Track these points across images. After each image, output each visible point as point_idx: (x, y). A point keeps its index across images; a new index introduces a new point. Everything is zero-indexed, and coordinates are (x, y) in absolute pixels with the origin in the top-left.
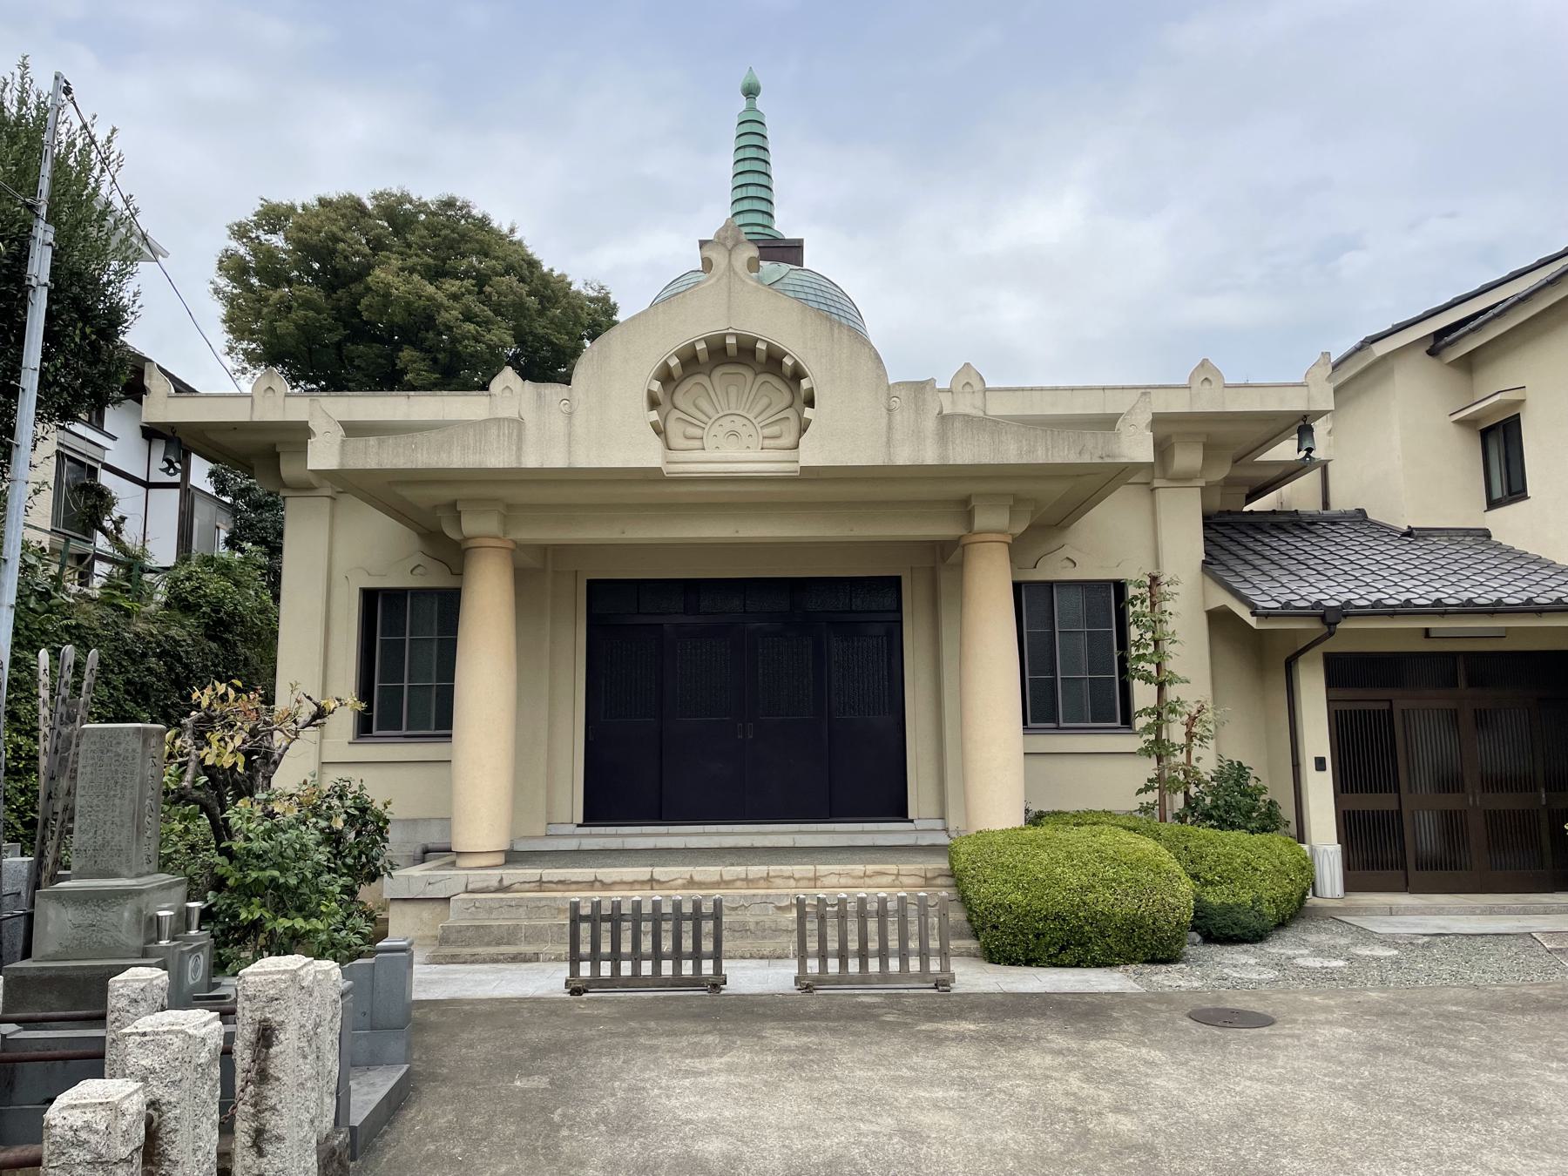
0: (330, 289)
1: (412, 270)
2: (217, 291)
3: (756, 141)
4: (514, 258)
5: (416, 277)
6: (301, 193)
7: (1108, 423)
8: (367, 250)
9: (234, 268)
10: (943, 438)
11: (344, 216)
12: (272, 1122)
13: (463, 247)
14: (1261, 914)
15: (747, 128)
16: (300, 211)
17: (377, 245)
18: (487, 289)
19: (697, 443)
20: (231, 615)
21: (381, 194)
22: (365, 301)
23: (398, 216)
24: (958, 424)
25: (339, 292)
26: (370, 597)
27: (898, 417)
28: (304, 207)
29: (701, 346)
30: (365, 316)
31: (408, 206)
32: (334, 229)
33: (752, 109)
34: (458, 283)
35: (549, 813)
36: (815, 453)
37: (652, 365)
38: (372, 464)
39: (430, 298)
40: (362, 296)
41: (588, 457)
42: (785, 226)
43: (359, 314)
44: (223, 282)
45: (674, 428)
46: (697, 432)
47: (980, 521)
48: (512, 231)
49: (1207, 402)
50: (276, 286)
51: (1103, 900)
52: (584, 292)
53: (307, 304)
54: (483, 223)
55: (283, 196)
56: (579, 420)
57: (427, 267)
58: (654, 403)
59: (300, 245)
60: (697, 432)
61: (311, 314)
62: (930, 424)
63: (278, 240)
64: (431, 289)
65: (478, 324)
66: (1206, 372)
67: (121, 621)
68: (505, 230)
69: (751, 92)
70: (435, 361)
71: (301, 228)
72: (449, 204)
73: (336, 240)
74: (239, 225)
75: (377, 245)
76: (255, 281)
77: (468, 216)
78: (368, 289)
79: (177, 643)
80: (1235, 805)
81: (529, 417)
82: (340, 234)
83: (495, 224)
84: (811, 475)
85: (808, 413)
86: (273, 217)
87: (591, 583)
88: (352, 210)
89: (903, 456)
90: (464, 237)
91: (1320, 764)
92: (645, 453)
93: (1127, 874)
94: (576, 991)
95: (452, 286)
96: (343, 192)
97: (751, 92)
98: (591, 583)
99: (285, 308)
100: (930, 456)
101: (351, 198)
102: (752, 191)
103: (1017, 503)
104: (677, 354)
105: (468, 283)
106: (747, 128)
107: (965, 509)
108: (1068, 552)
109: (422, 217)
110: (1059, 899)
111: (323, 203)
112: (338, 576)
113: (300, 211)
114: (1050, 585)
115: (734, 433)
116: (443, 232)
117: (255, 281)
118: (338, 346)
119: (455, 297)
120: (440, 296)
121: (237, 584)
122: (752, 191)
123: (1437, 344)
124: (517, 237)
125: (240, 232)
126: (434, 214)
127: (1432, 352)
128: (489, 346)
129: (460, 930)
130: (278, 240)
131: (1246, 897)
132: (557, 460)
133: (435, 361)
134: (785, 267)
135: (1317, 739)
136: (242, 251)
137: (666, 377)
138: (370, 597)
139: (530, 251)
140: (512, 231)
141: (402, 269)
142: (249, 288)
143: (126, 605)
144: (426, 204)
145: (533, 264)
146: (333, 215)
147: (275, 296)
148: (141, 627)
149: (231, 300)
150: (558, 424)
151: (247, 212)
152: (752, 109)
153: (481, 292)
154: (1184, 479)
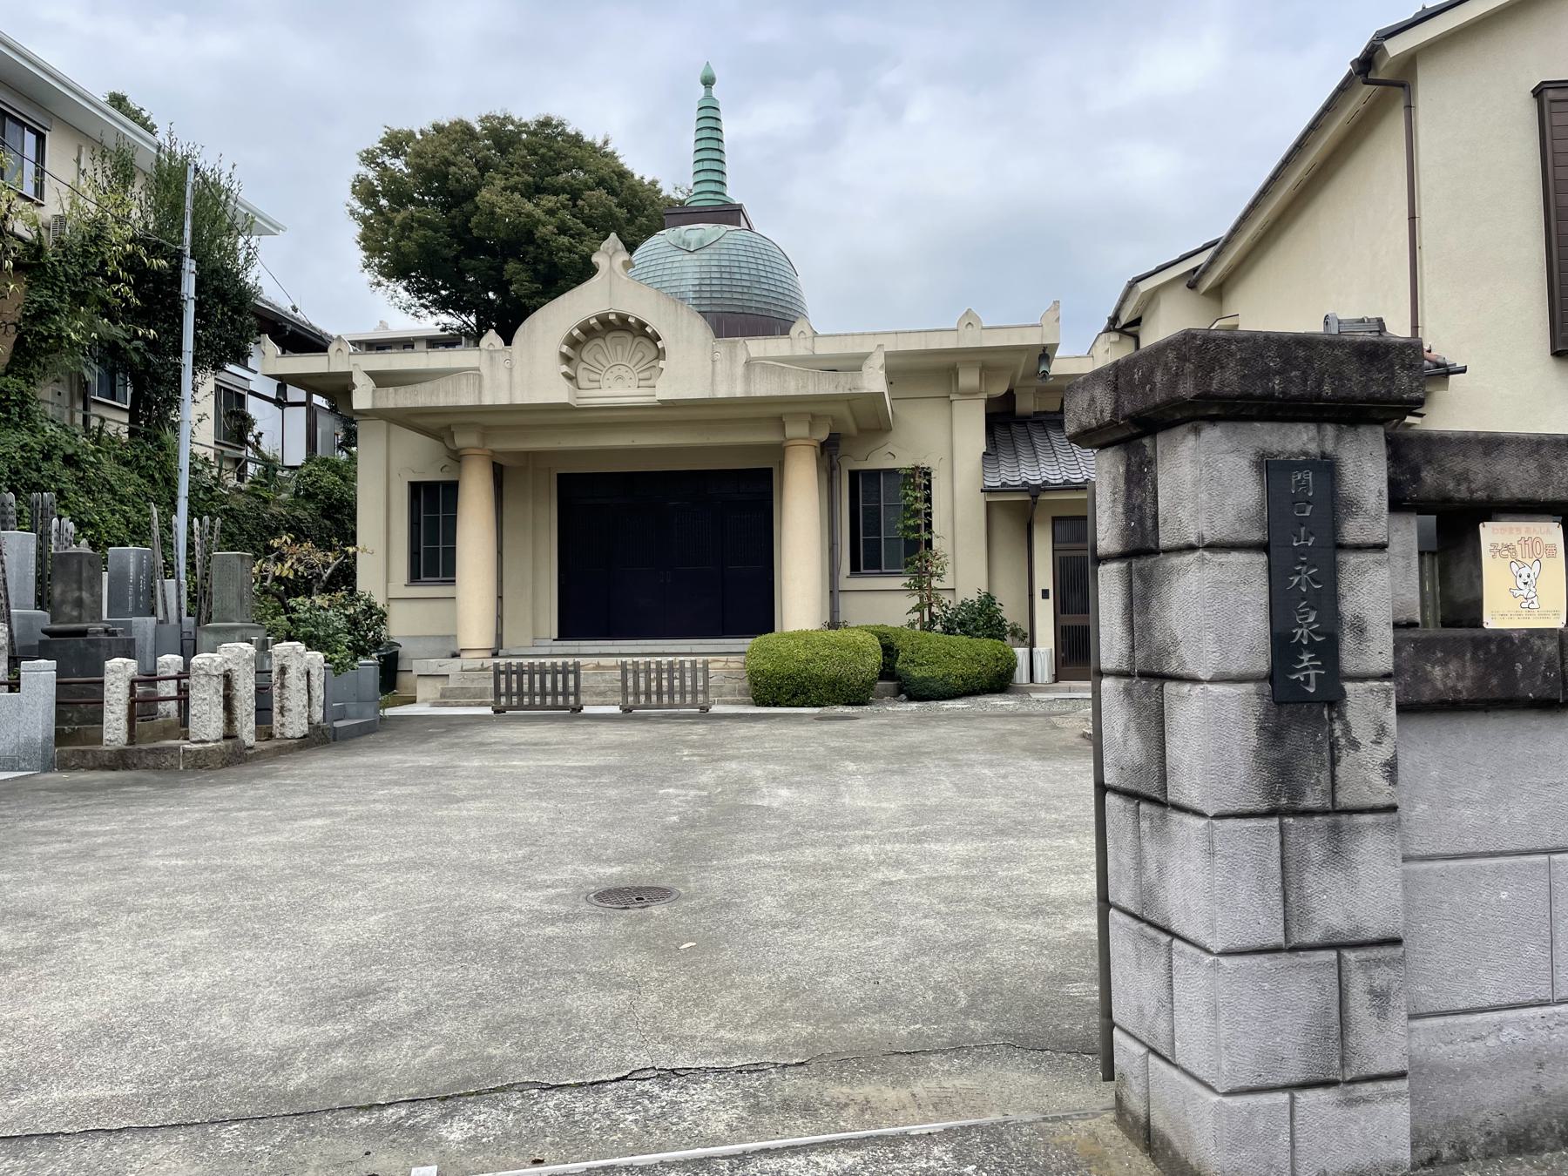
0: (446, 208)
1: (514, 189)
2: (352, 213)
3: (711, 123)
4: (605, 172)
5: (517, 196)
6: (419, 122)
7: (855, 364)
8: (475, 172)
9: (365, 192)
10: (747, 379)
11: (454, 141)
12: (287, 703)
13: (559, 165)
14: (947, 684)
15: (703, 113)
16: (419, 137)
17: (484, 166)
18: (580, 203)
19: (596, 385)
20: (340, 501)
21: (487, 117)
22: (474, 220)
23: (502, 136)
24: (758, 370)
25: (453, 212)
26: (415, 487)
27: (718, 365)
28: (422, 132)
29: (576, 332)
30: (475, 232)
31: (511, 127)
32: (446, 153)
33: (709, 96)
34: (554, 198)
35: (535, 628)
36: (666, 390)
37: (562, 334)
38: (391, 405)
39: (529, 215)
40: (473, 214)
41: (522, 398)
42: (733, 194)
43: (469, 231)
44: (356, 204)
45: (582, 376)
46: (597, 377)
47: (792, 430)
48: (606, 143)
49: (970, 340)
50: (403, 206)
51: (817, 668)
52: (674, 196)
53: (424, 223)
54: (577, 140)
55: (402, 124)
56: (516, 373)
57: (527, 185)
58: (567, 359)
59: (418, 169)
60: (597, 377)
61: (430, 233)
62: (740, 370)
63: (399, 164)
64: (529, 207)
65: (572, 236)
66: (970, 319)
67: (261, 506)
68: (599, 143)
69: (708, 82)
70: (535, 270)
71: (419, 155)
72: (546, 123)
73: (448, 163)
74: (367, 152)
75: (484, 166)
76: (383, 202)
77: (563, 133)
78: (477, 207)
79: (301, 521)
80: (983, 619)
81: (485, 371)
82: (451, 158)
83: (587, 138)
84: (667, 405)
85: (662, 364)
86: (395, 143)
87: (560, 476)
88: (462, 133)
89: (722, 392)
90: (559, 155)
91: (1045, 594)
92: (560, 393)
93: (837, 652)
94: (496, 712)
95: (549, 201)
96: (454, 118)
97: (708, 82)
98: (560, 476)
99: (406, 227)
100: (739, 392)
101: (460, 122)
102: (707, 165)
103: (814, 420)
104: (578, 327)
105: (563, 197)
106: (703, 113)
107: (779, 422)
108: (885, 450)
109: (524, 136)
110: (792, 666)
111: (438, 129)
112: (394, 474)
113: (419, 137)
114: (879, 471)
115: (620, 377)
116: (543, 150)
117: (383, 202)
118: (457, 258)
119: (551, 212)
120: (538, 213)
121: (344, 478)
122: (707, 165)
123: (1192, 280)
124: (609, 149)
125: (369, 158)
126: (534, 133)
127: (1192, 286)
128: (581, 257)
129: (452, 690)
130: (399, 164)
131: (939, 672)
132: (503, 399)
133: (535, 270)
134: (724, 228)
135: (1044, 578)
136: (371, 175)
137: (573, 343)
138: (415, 487)
139: (621, 161)
140: (606, 143)
141: (505, 189)
142: (379, 211)
143: (264, 495)
144: (526, 125)
145: (623, 175)
146: (445, 141)
147: (398, 218)
148: (275, 510)
149: (364, 220)
150: (503, 376)
151: (374, 143)
152: (709, 96)
153: (575, 206)
154: (970, 394)
